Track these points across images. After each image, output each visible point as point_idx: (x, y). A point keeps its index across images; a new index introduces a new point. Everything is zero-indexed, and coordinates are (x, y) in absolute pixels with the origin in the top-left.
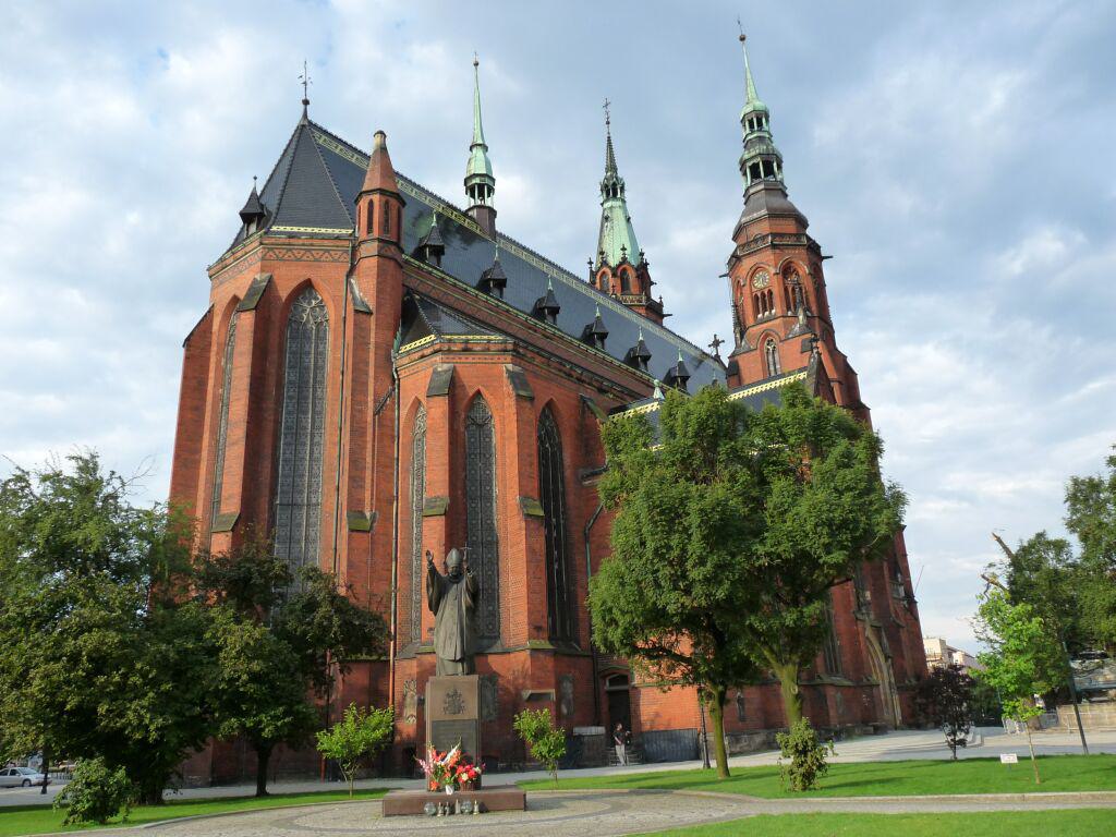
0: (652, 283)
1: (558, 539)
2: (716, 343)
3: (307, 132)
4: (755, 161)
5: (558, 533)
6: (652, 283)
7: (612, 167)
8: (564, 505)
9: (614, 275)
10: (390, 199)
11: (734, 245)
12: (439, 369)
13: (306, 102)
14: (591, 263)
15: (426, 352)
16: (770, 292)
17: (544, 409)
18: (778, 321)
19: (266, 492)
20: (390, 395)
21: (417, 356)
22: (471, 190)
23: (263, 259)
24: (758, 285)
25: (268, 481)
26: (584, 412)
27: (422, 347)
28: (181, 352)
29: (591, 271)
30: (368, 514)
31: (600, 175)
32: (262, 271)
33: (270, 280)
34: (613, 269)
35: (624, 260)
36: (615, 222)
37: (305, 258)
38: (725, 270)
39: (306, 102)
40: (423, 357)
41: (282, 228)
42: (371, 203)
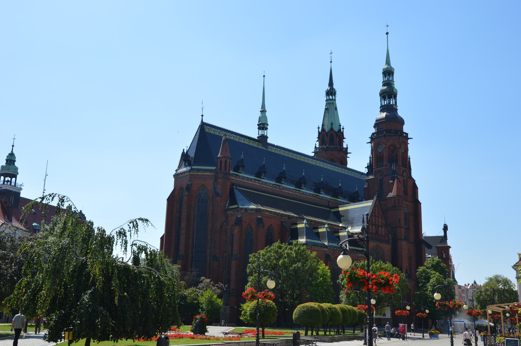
0: (344, 138)
3: (203, 126)
4: (385, 94)
6: (344, 138)
7: (331, 84)
9: (327, 136)
11: (374, 130)
12: (238, 217)
13: (202, 116)
14: (319, 128)
16: (383, 154)
17: (269, 226)
18: (384, 168)
20: (224, 222)
22: (259, 128)
23: (190, 178)
24: (380, 150)
29: (319, 132)
30: (218, 256)
31: (327, 87)
34: (327, 133)
35: (332, 129)
38: (369, 140)
39: (202, 116)
42: (221, 160)
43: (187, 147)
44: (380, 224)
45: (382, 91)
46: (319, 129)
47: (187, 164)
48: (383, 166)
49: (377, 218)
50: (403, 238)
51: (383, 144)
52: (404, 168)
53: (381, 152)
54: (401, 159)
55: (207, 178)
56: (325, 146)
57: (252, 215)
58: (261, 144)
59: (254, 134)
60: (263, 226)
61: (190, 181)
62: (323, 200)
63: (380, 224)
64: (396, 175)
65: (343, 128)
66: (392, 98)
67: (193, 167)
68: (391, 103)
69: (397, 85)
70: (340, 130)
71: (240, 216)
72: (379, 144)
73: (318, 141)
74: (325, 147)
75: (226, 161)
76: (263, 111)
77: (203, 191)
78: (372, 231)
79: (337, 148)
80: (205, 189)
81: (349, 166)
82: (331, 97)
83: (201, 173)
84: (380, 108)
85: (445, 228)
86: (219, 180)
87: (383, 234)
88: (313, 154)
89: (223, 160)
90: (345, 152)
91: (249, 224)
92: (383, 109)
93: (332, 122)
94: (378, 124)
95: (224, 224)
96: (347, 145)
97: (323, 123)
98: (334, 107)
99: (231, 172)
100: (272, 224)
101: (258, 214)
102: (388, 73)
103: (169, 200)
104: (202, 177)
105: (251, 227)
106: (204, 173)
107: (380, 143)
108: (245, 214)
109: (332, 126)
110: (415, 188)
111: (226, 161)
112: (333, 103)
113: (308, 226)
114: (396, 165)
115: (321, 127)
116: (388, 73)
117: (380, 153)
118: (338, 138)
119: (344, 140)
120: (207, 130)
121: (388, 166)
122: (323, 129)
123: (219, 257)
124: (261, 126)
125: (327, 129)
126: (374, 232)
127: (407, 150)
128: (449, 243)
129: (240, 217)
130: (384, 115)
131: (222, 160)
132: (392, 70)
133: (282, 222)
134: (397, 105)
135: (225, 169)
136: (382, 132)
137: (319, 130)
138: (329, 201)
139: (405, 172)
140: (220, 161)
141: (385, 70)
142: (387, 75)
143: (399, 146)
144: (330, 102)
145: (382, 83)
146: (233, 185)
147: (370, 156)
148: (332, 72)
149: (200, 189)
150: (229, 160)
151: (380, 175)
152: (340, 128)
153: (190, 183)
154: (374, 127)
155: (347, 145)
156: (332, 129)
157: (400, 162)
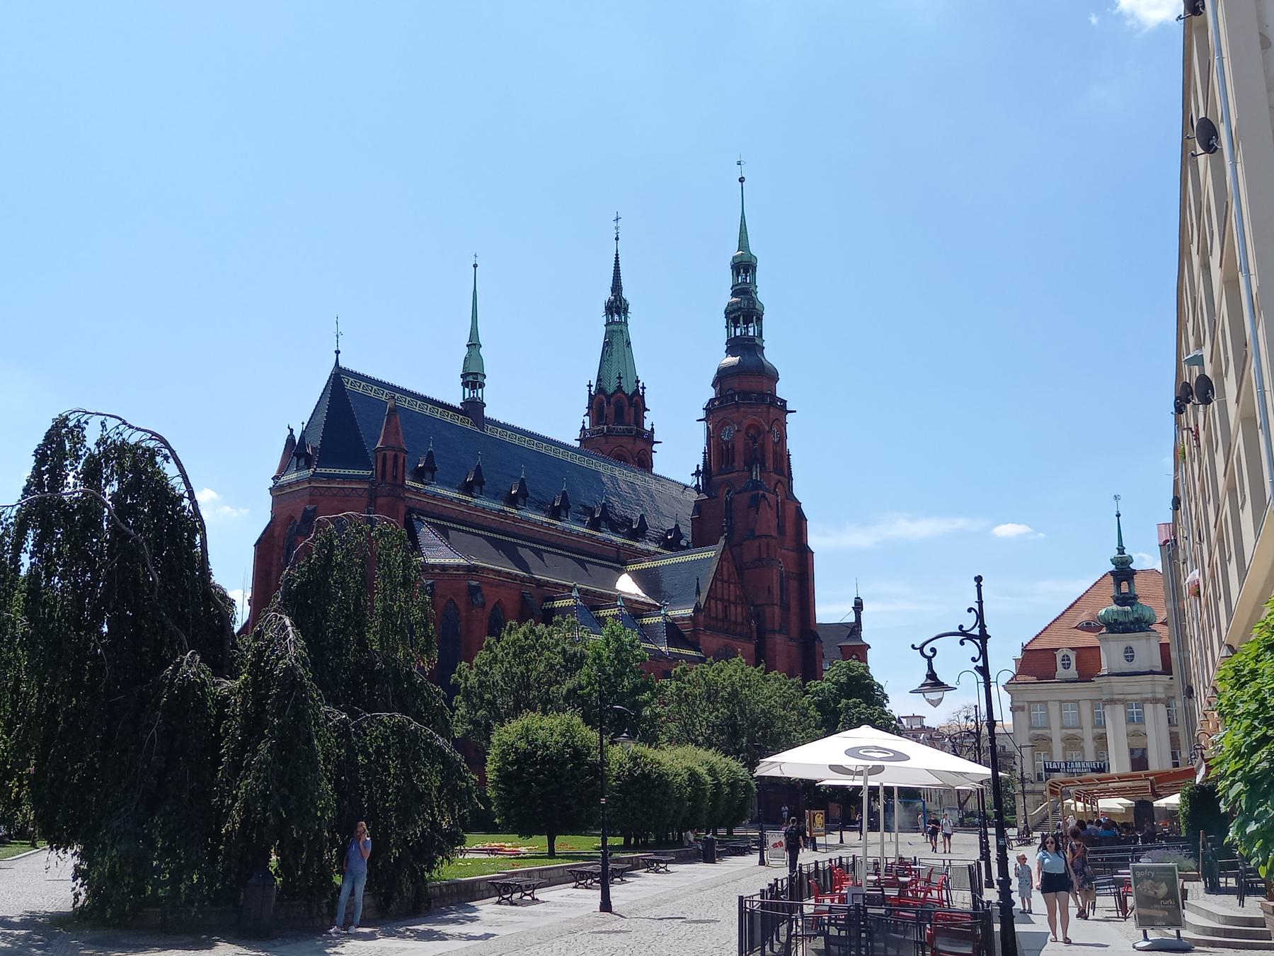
0: (647, 410)
2: (697, 473)
4: (736, 314)
6: (647, 410)
7: (617, 287)
9: (609, 403)
10: (398, 453)
13: (338, 352)
14: (590, 386)
16: (733, 445)
17: (495, 605)
18: (734, 475)
22: (465, 384)
23: (311, 495)
29: (590, 393)
31: (607, 295)
35: (620, 388)
37: (339, 494)
38: (702, 415)
39: (338, 352)
41: (323, 470)
43: (303, 423)
44: (732, 598)
45: (730, 305)
46: (590, 388)
47: (302, 463)
48: (733, 472)
49: (726, 585)
50: (777, 627)
51: (734, 423)
52: (777, 477)
53: (728, 442)
54: (771, 456)
55: (351, 495)
56: (605, 427)
58: (470, 420)
59: (454, 395)
60: (484, 605)
61: (311, 503)
62: (607, 546)
63: (732, 598)
64: (761, 492)
65: (643, 388)
66: (752, 322)
67: (318, 470)
68: (751, 334)
69: (764, 293)
70: (637, 390)
72: (726, 422)
73: (587, 415)
74: (605, 429)
75: (396, 457)
76: (474, 344)
78: (717, 613)
79: (630, 431)
81: (653, 472)
82: (616, 318)
83: (338, 484)
84: (726, 344)
85: (858, 606)
86: (381, 501)
87: (740, 620)
88: (577, 444)
89: (390, 454)
90: (648, 439)
91: (451, 599)
92: (734, 346)
94: (723, 377)
96: (652, 425)
97: (599, 375)
99: (410, 483)
101: (471, 576)
102: (744, 267)
103: (260, 545)
104: (339, 494)
105: (456, 607)
106: (344, 484)
107: (728, 421)
109: (620, 383)
110: (800, 519)
111: (396, 457)
112: (621, 331)
113: (580, 603)
114: (761, 470)
115: (594, 383)
116: (744, 267)
117: (726, 442)
118: (633, 409)
119: (646, 414)
120: (348, 387)
121: (744, 471)
122: (600, 390)
124: (470, 378)
125: (610, 390)
126: (720, 615)
127: (783, 438)
128: (866, 636)
130: (733, 360)
131: (388, 455)
132: (753, 260)
133: (523, 597)
134: (763, 338)
135: (395, 478)
136: (732, 396)
137: (590, 391)
138: (618, 547)
139: (779, 485)
140: (382, 456)
141: (736, 261)
142: (742, 271)
143: (767, 428)
144: (614, 327)
145: (732, 289)
146: (410, 511)
147: (705, 450)
150: (403, 455)
151: (725, 492)
152: (638, 386)
154: (714, 385)
155: (652, 425)
156: (620, 388)
157: (770, 464)
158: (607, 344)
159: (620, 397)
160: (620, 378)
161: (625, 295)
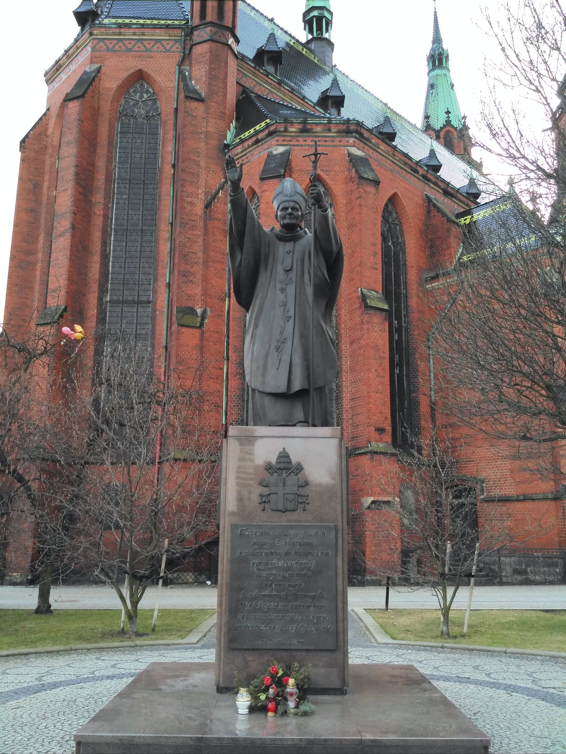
1: (399, 342)
5: (400, 336)
7: (437, 39)
8: (407, 306)
12: (275, 152)
15: (260, 136)
17: (386, 205)
19: (95, 287)
21: (250, 142)
22: (308, 23)
25: (97, 276)
26: (429, 212)
27: (257, 133)
28: (17, 156)
30: (199, 311)
32: (92, 62)
33: (99, 70)
35: (448, 122)
36: (440, 89)
37: (136, 48)
40: (257, 141)
57: (327, 143)
71: (281, 149)
77: (142, 97)
80: (147, 92)
93: (448, 108)
95: (220, 195)
98: (449, 83)
100: (399, 193)
108: (300, 143)
109: (449, 117)
112: (445, 75)
123: (204, 313)
129: (282, 154)
148: (437, 20)
149: (132, 90)
153: (95, 66)
156: (448, 122)
158: (432, 86)
159: (448, 131)
160: (448, 112)
161: (445, 45)
